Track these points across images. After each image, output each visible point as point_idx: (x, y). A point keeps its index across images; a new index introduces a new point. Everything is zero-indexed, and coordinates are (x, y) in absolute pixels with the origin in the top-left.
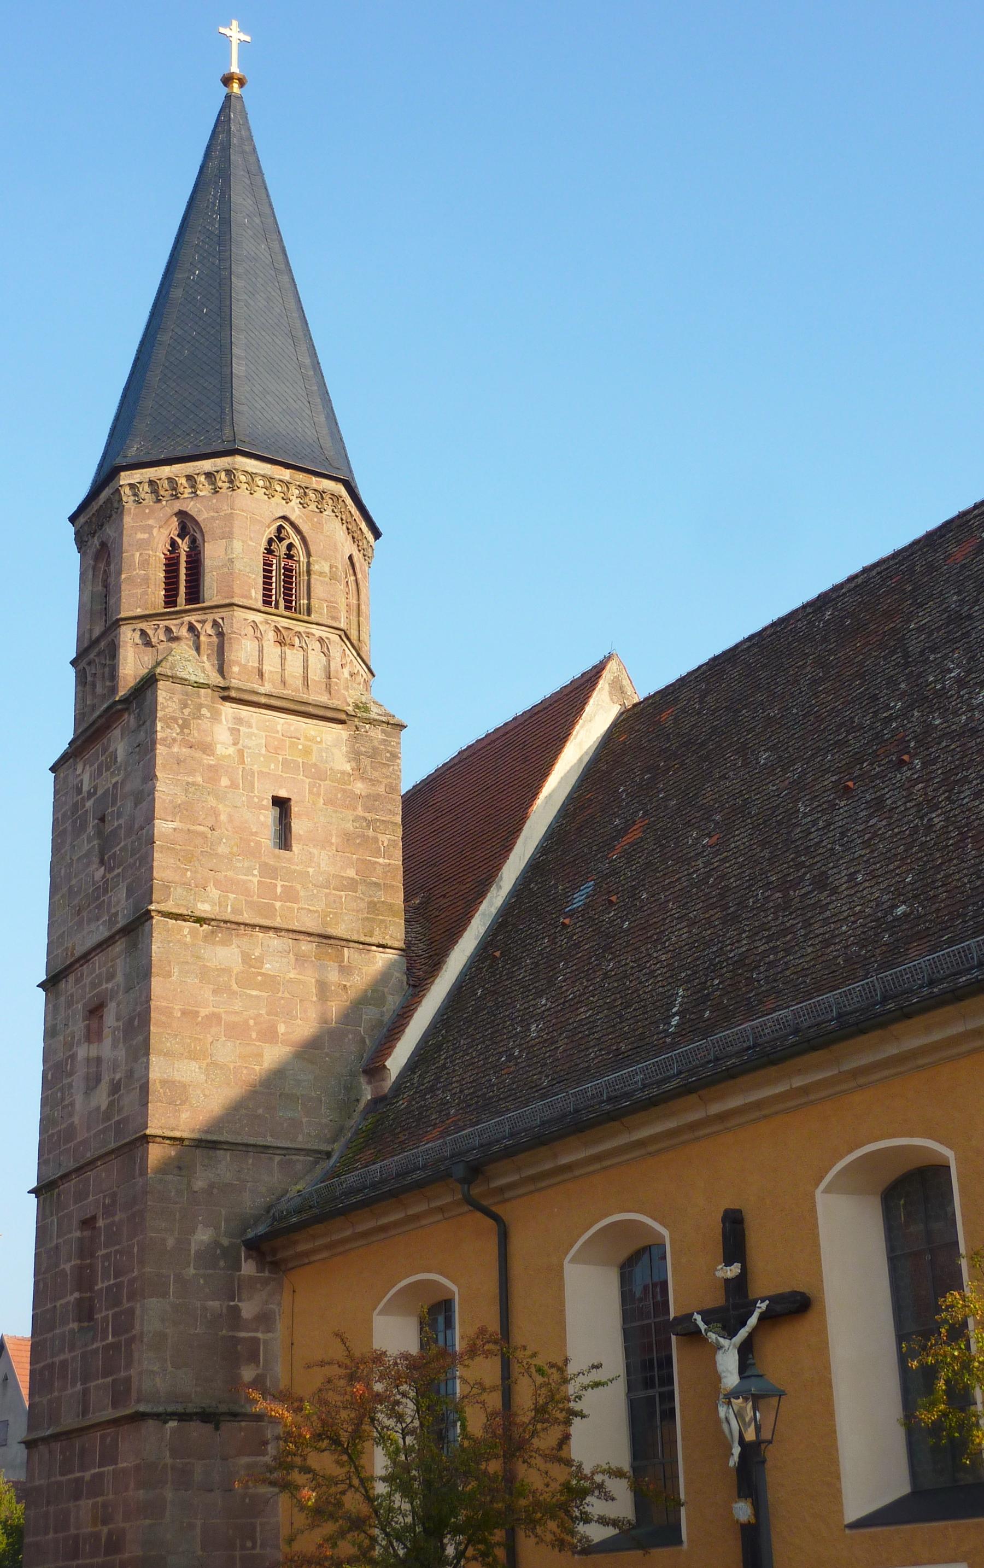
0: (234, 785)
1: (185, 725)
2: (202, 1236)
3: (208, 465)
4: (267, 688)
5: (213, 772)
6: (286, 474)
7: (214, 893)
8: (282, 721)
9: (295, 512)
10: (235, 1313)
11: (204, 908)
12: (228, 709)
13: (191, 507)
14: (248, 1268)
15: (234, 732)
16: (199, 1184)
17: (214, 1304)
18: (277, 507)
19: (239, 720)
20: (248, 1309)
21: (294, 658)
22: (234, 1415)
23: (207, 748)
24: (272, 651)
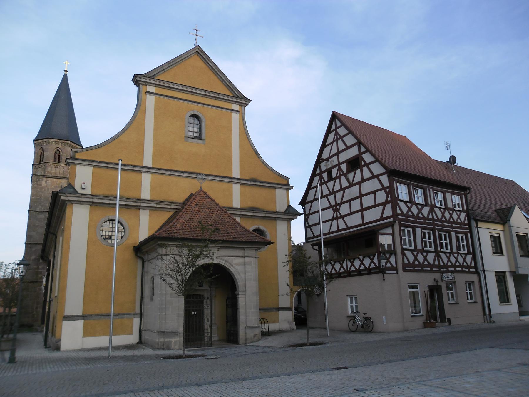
0: (45, 190)
1: (37, 182)
2: (33, 257)
3: (45, 140)
4: (52, 175)
5: (42, 188)
6: (58, 141)
7: (40, 207)
8: (55, 180)
9: (60, 146)
10: (38, 268)
11: (38, 209)
12: (45, 179)
13: (43, 147)
14: (41, 261)
15: (46, 182)
16: (34, 249)
17: (35, 267)
18: (57, 146)
19: (47, 180)
20: (40, 267)
21: (58, 170)
22: (37, 282)
23: (41, 185)
24: (54, 169)
